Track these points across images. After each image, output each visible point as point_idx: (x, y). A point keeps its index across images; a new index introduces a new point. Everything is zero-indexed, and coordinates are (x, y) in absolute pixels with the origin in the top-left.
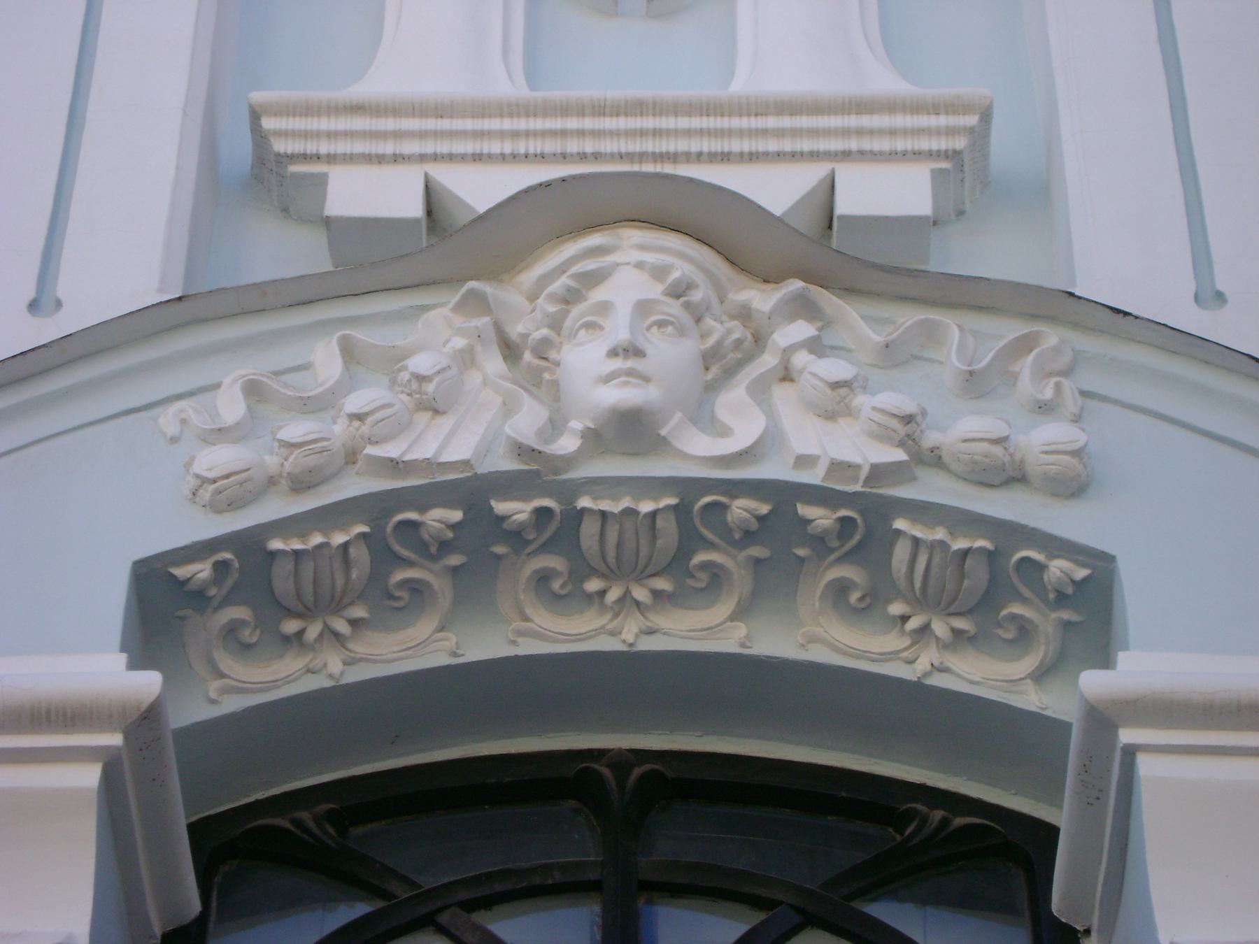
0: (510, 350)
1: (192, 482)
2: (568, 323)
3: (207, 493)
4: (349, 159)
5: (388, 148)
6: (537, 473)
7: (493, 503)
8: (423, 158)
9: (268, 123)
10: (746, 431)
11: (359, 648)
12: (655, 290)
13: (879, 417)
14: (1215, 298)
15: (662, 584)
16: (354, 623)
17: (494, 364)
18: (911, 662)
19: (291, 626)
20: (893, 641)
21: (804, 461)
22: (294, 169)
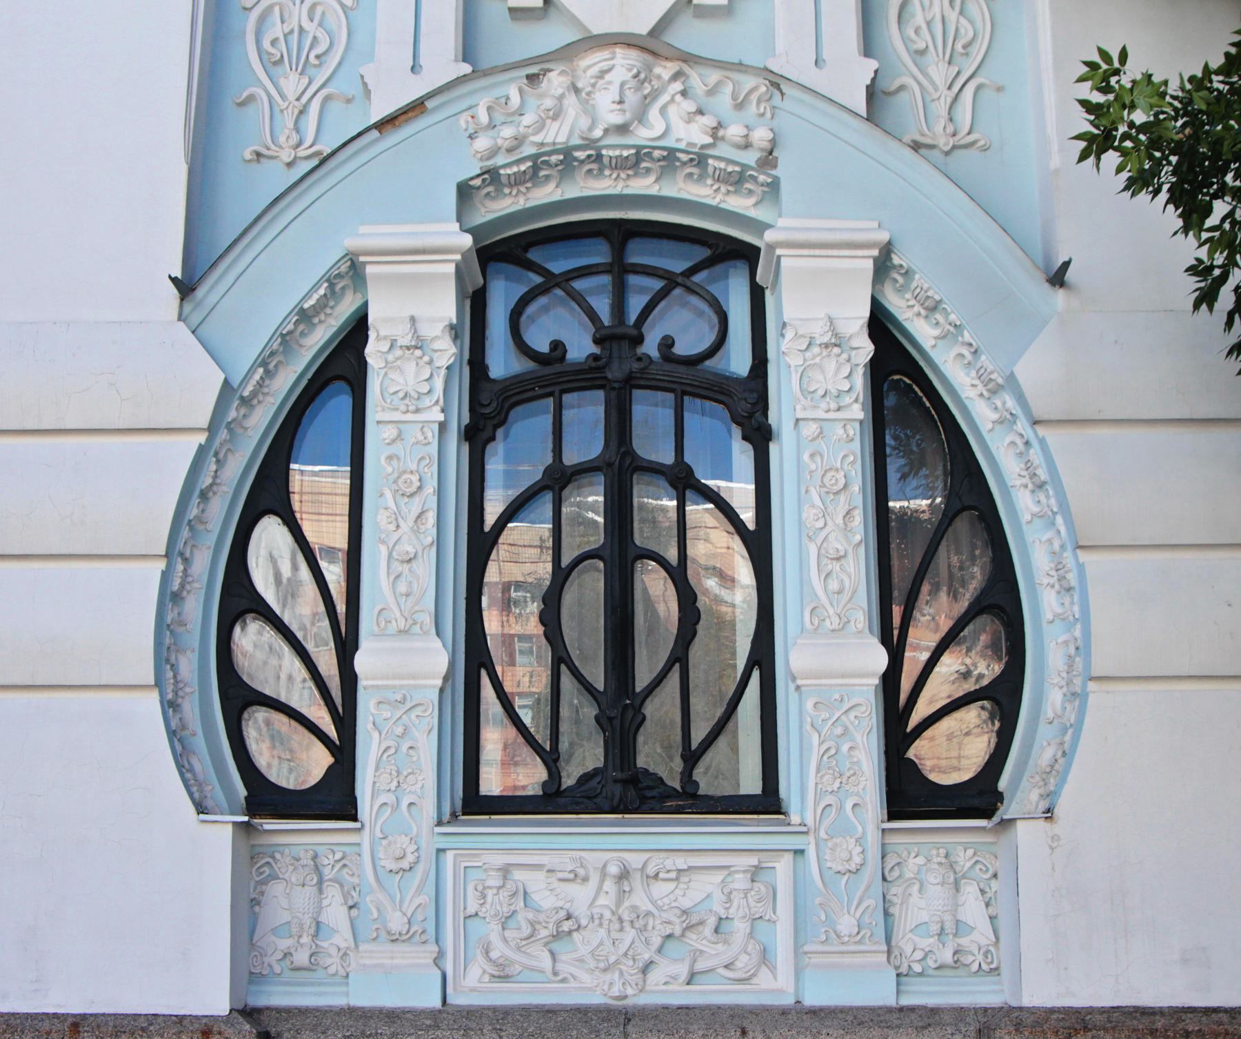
1: (474, 152)
2: (598, 86)
3: (479, 156)
10: (659, 128)
11: (530, 195)
15: (630, 172)
18: (714, 198)
20: (709, 191)
21: (678, 140)
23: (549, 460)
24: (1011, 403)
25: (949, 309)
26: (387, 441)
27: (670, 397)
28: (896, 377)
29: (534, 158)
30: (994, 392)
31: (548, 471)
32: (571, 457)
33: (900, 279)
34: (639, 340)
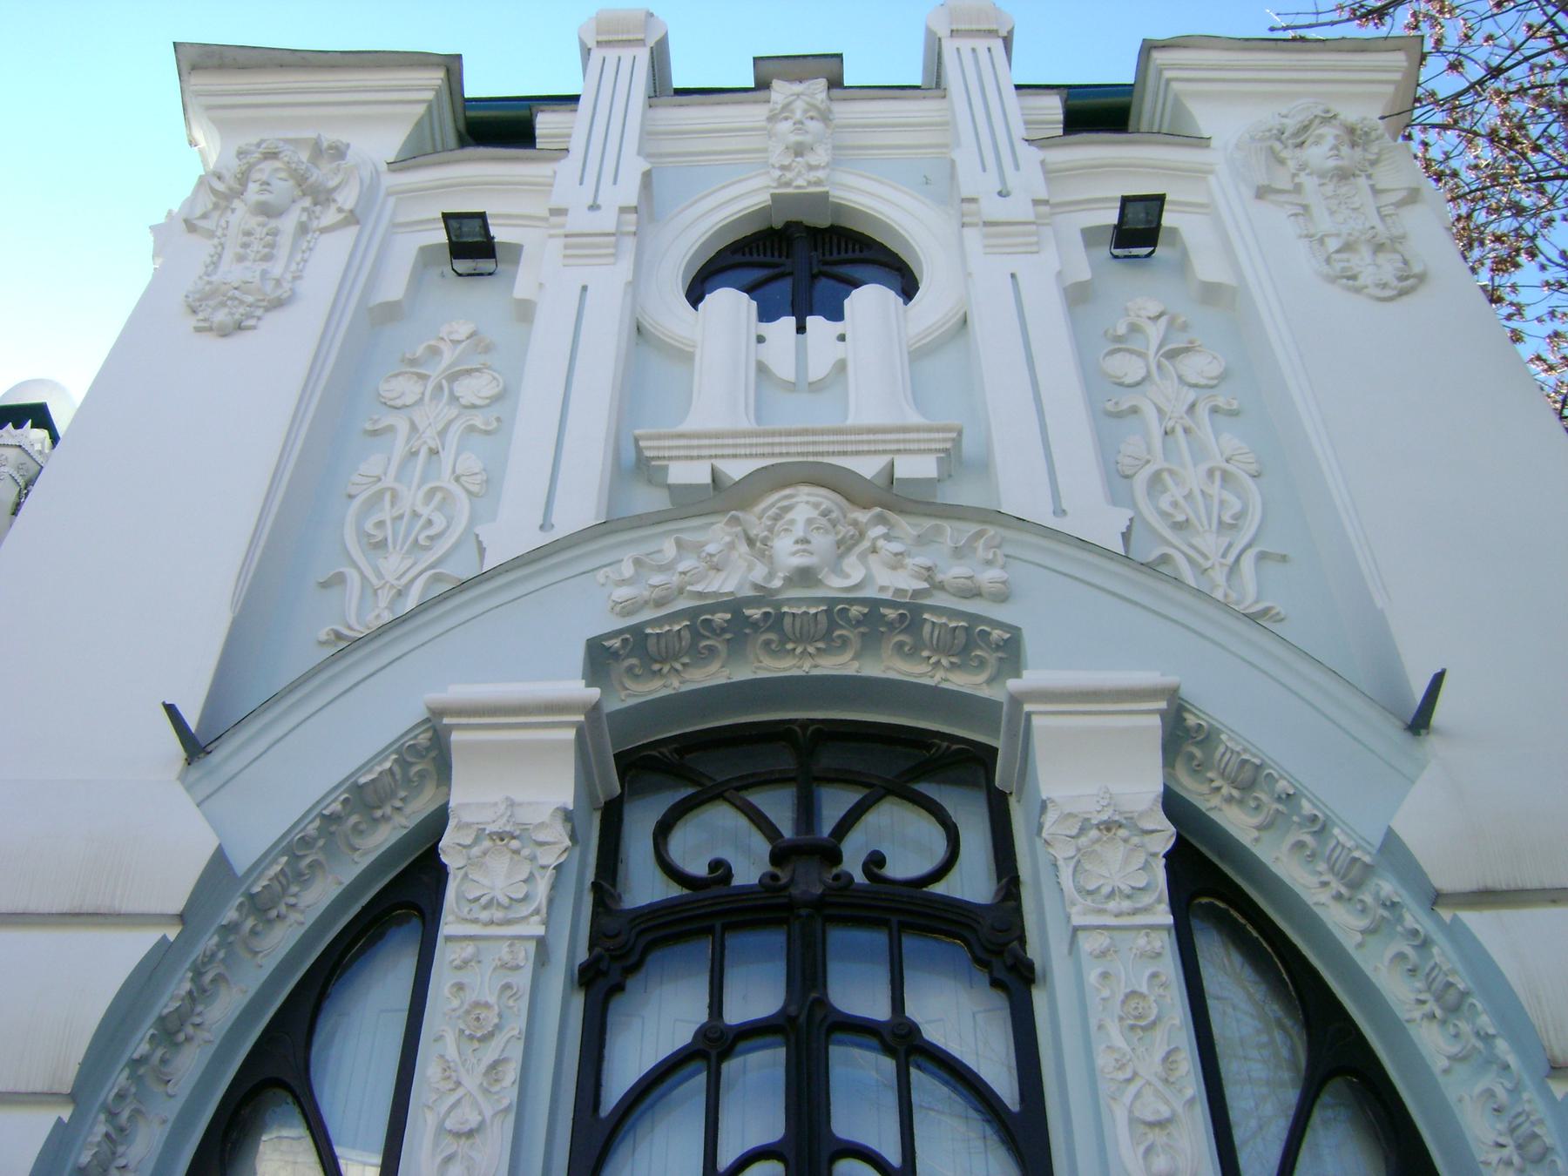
0: (751, 542)
2: (776, 528)
3: (618, 608)
4: (678, 458)
5: (695, 453)
6: (764, 596)
7: (744, 610)
8: (711, 457)
9: (642, 444)
10: (856, 576)
11: (687, 676)
12: (814, 514)
13: (916, 569)
14: (1060, 512)
15: (821, 645)
16: (684, 665)
17: (743, 548)
18: (932, 677)
19: (656, 667)
20: (924, 668)
21: (882, 589)
22: (653, 463)
23: (702, 1016)
24: (1387, 886)
25: (1276, 775)
26: (456, 963)
27: (880, 938)
28: (1204, 900)
29: (692, 613)
30: (1355, 885)
31: (703, 1033)
32: (736, 1013)
33: (1198, 752)
34: (832, 855)
